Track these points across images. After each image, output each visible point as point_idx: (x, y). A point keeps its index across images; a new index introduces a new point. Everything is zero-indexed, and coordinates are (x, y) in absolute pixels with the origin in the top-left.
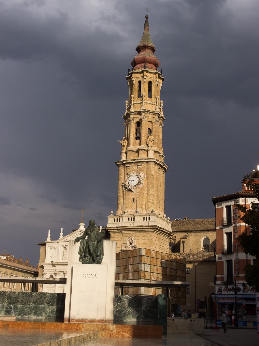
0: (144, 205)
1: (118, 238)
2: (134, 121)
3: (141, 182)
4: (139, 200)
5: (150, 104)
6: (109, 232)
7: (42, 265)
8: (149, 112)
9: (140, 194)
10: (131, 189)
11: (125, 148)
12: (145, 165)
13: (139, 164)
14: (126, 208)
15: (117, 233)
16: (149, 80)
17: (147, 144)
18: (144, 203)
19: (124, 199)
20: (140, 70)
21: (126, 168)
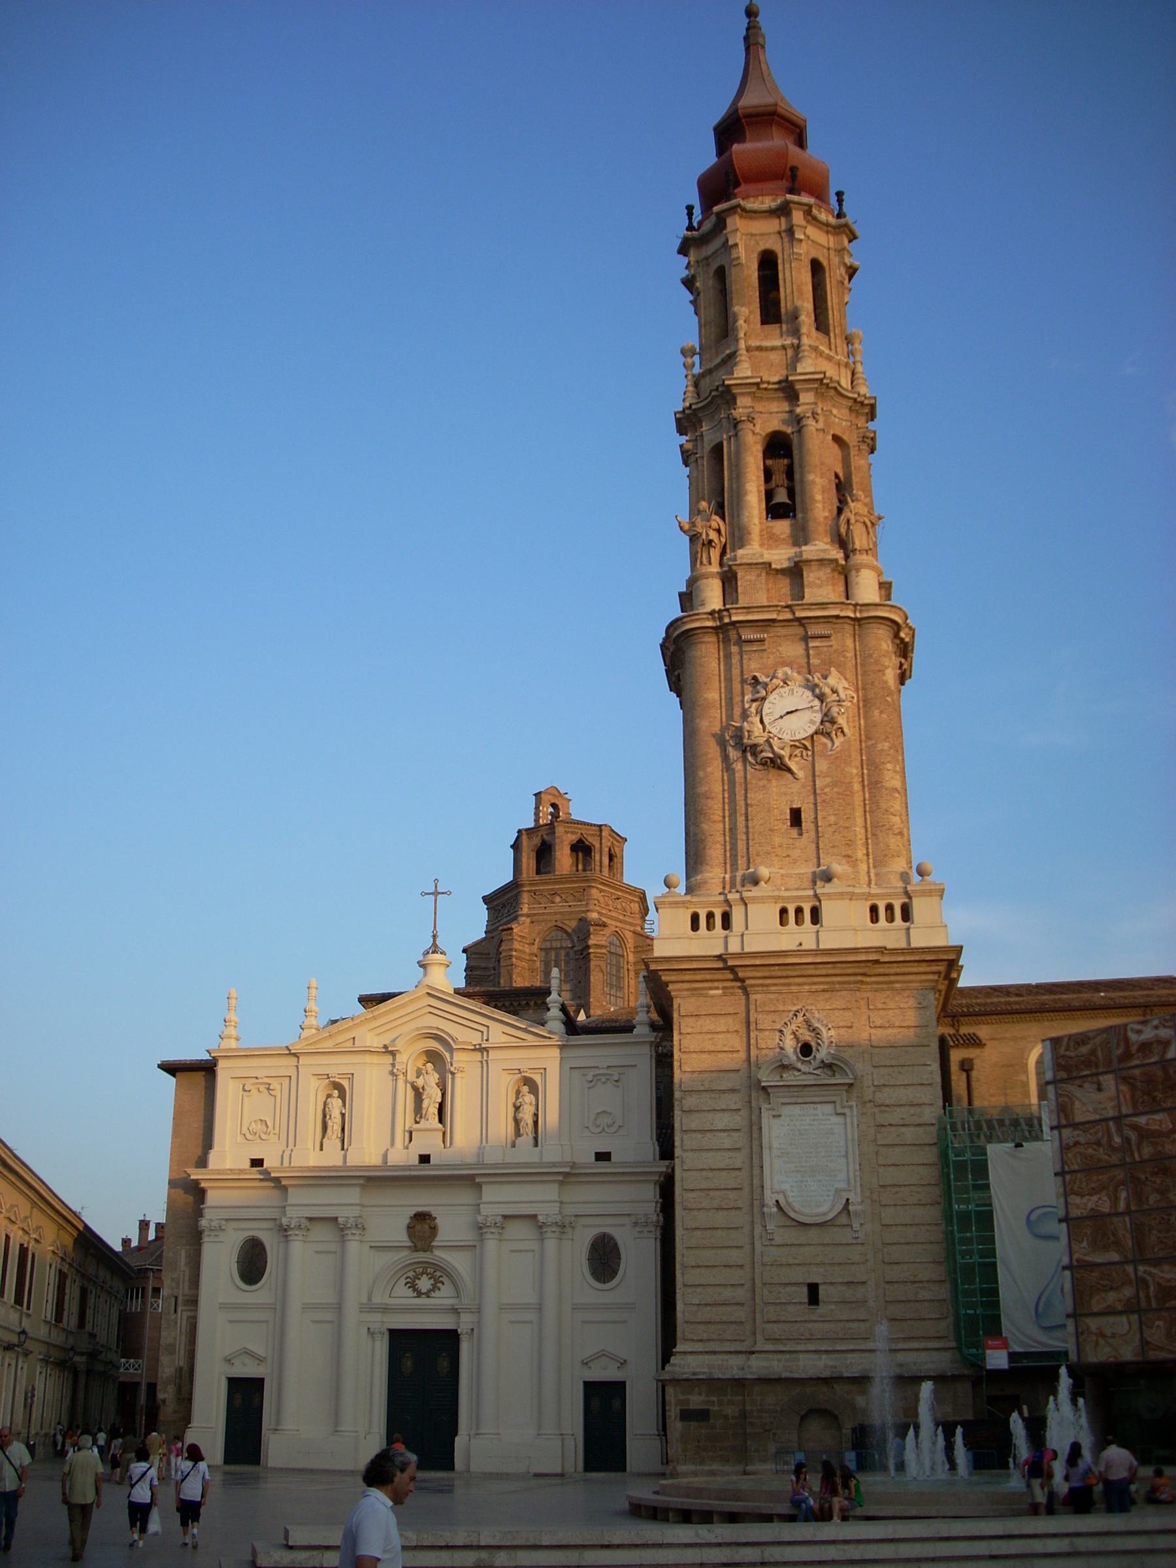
0: (859, 843)
1: (722, 1020)
2: (758, 427)
3: (842, 721)
4: (832, 819)
5: (829, 358)
6: (667, 984)
7: (197, 1182)
8: (835, 388)
9: (835, 784)
10: (781, 758)
11: (715, 554)
12: (844, 641)
13: (813, 630)
14: (758, 860)
15: (712, 992)
16: (814, 254)
17: (843, 542)
18: (859, 830)
19: (741, 808)
20: (767, 203)
21: (734, 649)
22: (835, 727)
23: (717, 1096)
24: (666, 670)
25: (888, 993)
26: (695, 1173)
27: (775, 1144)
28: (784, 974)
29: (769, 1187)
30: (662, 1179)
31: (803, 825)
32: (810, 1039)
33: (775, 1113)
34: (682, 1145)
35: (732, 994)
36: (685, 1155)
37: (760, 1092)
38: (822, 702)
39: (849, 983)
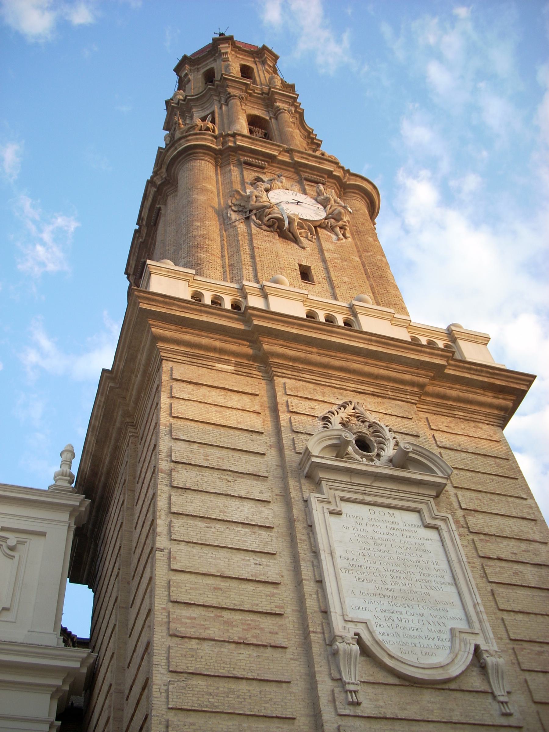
6: (157, 338)
15: (219, 366)
22: (341, 223)
23: (230, 479)
24: (136, 231)
25: (450, 419)
26: (192, 578)
27: (338, 552)
28: (325, 360)
29: (339, 610)
30: (67, 688)
31: (315, 278)
32: (365, 431)
33: (333, 507)
34: (170, 532)
35: (249, 375)
36: (175, 548)
37: (303, 481)
38: (325, 208)
39: (405, 392)
